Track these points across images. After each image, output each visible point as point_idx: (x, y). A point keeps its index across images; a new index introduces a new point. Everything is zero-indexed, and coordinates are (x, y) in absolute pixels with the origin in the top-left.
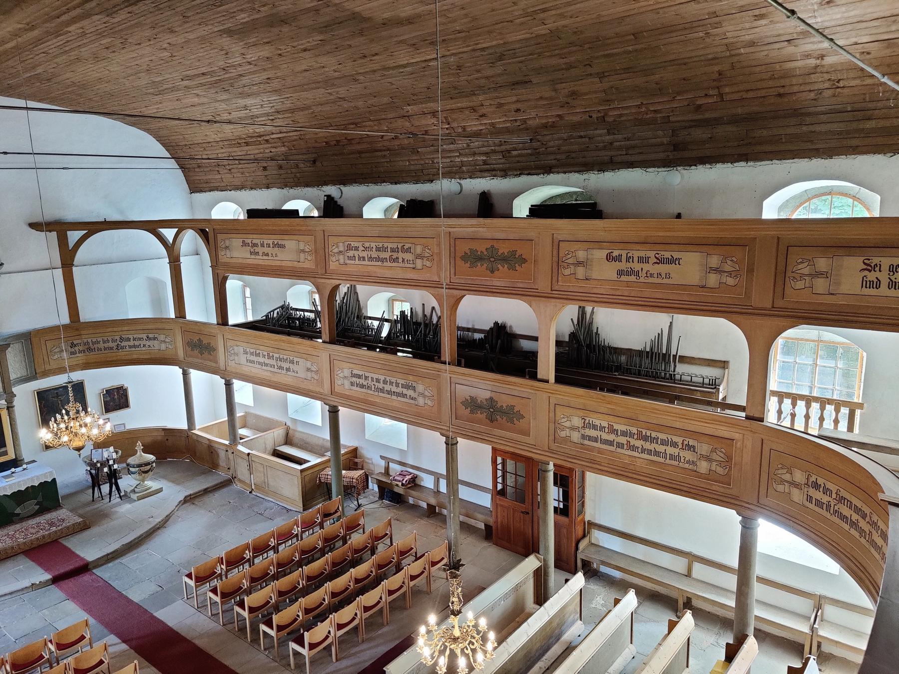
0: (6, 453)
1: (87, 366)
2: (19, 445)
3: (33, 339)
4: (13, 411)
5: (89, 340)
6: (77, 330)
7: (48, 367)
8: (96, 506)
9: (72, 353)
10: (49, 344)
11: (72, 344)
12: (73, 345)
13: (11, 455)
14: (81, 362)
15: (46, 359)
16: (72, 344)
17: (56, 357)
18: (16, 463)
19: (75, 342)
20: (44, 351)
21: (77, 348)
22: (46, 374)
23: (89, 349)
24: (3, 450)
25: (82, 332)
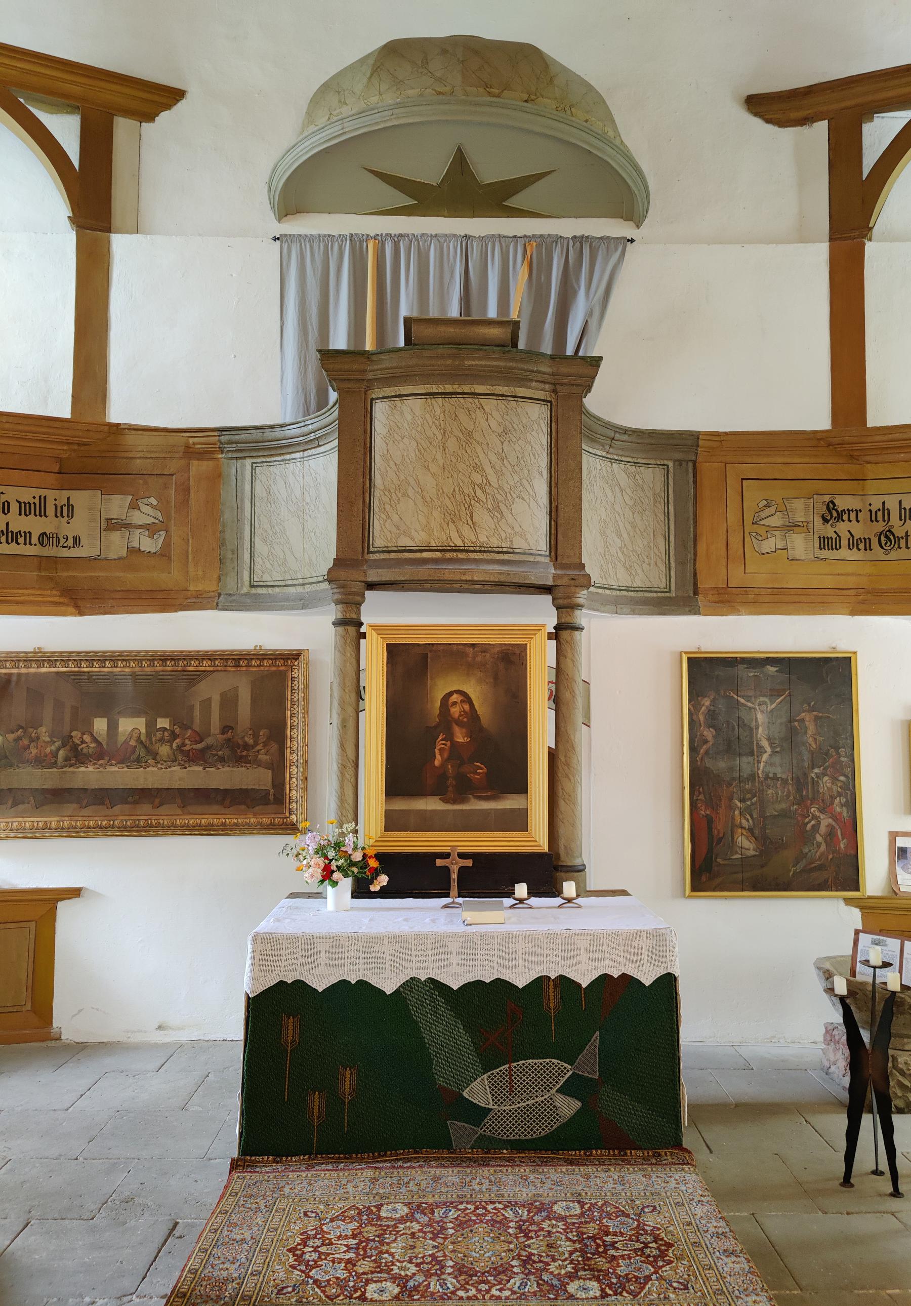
0: (518, 821)
1: (871, 600)
2: (572, 800)
3: (704, 467)
4: (572, 643)
5: (892, 503)
6: (852, 458)
7: (737, 577)
8: (864, 1224)
9: (826, 543)
10: (754, 495)
11: (831, 506)
12: (832, 514)
13: (537, 837)
14: (852, 582)
15: (735, 541)
16: (831, 506)
17: (769, 545)
18: (545, 873)
19: (842, 503)
20: (733, 517)
21: (843, 527)
22: (729, 600)
23: (888, 538)
24: (510, 803)
25: (871, 471)
